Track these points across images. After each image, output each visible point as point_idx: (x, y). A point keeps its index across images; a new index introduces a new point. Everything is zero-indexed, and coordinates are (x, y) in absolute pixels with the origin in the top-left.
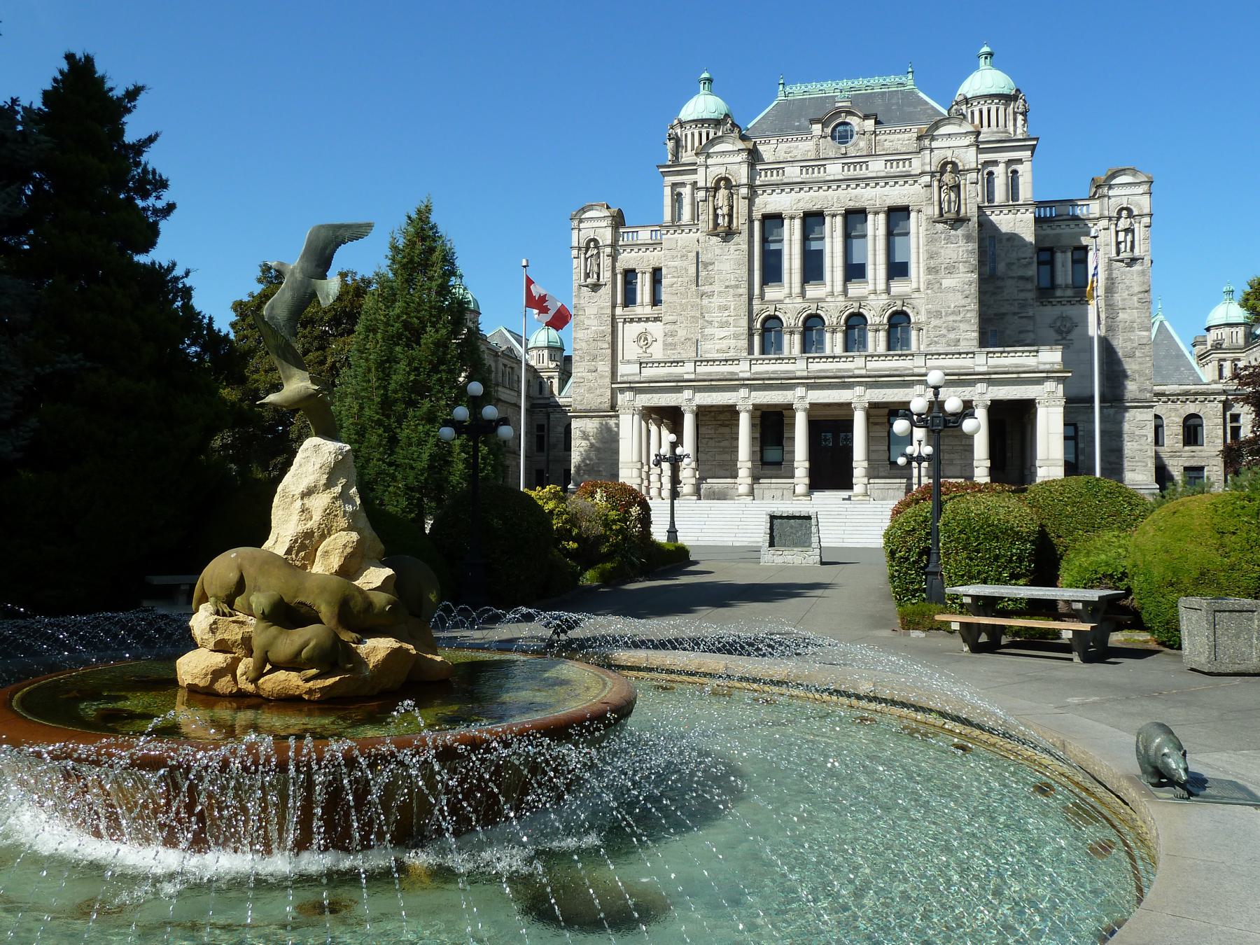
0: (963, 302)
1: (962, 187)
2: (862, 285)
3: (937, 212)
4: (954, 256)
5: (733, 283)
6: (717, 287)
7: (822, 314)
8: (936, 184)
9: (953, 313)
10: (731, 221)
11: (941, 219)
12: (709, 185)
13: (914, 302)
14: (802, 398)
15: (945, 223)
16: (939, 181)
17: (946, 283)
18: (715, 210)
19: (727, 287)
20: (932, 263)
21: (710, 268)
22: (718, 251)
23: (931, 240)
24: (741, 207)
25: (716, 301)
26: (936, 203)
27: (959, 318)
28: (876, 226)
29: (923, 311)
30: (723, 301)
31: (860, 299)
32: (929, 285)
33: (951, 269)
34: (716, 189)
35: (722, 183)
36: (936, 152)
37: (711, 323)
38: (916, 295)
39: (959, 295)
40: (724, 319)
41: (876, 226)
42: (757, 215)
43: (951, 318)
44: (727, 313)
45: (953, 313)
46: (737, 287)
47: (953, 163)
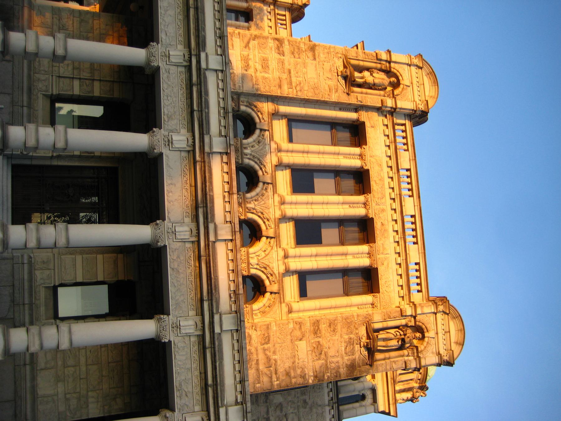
0: (281, 370)
1: (401, 352)
2: (292, 241)
3: (377, 326)
4: (331, 352)
5: (294, 79)
6: (288, 59)
7: (258, 190)
8: (403, 322)
9: (268, 359)
10: (360, 86)
11: (372, 333)
12: (392, 65)
13: (276, 307)
14: (169, 142)
15: (368, 337)
16: (406, 326)
17: (303, 346)
18: (368, 69)
19: (290, 72)
20: (323, 326)
21: (310, 54)
22: (327, 66)
23: (348, 322)
24: (372, 98)
25: (273, 57)
26: (385, 325)
27: (261, 367)
28: (356, 256)
29: (267, 319)
30: (273, 64)
31: (276, 237)
32: (300, 324)
33: (318, 350)
34: (388, 72)
35: (393, 79)
36: (432, 317)
37: (247, 46)
38: (285, 309)
39: (288, 364)
40: (251, 63)
41: (356, 256)
42: (364, 116)
43: (261, 357)
44: (259, 67)
45: (268, 359)
46: (291, 83)
47: (423, 337)
